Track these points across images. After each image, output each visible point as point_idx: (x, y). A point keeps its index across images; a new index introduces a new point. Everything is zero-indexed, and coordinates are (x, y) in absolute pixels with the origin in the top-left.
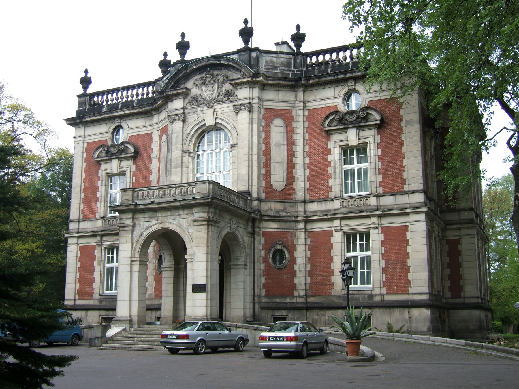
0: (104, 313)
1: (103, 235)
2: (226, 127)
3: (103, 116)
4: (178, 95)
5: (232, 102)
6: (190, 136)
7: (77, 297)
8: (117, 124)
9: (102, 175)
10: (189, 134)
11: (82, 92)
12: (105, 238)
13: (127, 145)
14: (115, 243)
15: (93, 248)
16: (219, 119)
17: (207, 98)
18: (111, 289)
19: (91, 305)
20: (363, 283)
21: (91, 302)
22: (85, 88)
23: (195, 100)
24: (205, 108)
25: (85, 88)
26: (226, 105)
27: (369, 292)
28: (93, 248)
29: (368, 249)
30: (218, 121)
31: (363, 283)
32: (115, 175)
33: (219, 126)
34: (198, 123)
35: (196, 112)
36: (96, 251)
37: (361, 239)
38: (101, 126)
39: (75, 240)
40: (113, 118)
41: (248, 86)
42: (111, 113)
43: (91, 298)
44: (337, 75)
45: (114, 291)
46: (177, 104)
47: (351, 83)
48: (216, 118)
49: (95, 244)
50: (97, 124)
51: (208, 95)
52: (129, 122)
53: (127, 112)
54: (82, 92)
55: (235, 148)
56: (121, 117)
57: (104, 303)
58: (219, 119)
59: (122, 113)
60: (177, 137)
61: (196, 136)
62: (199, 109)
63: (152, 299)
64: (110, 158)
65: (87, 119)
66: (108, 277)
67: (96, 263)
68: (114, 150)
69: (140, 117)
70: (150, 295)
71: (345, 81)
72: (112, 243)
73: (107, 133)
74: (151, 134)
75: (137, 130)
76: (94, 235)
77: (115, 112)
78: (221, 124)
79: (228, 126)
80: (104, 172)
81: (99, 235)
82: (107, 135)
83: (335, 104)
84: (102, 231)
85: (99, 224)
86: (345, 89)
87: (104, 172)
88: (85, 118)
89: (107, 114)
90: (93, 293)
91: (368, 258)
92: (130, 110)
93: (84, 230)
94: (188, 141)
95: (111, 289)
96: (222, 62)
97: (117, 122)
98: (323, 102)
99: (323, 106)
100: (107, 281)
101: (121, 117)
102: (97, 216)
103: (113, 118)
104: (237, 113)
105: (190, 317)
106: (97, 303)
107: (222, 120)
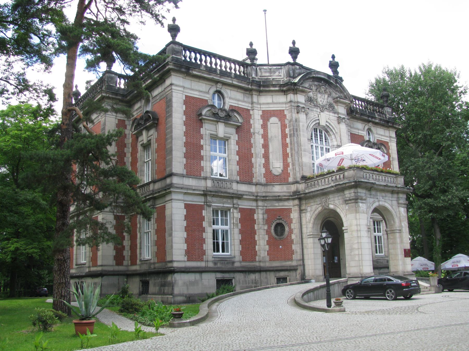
0: (219, 276)
1: (214, 196)
3: (212, 77)
4: (303, 91)
5: (335, 113)
7: (186, 259)
8: (218, 89)
9: (206, 134)
11: (170, 39)
12: (215, 199)
13: (236, 114)
14: (224, 205)
15: (201, 208)
17: (321, 103)
18: (218, 251)
19: (202, 268)
20: (380, 253)
21: (203, 264)
22: (174, 36)
23: (310, 100)
24: (319, 110)
25: (174, 36)
26: (331, 114)
27: (386, 258)
28: (201, 208)
29: (380, 232)
31: (380, 253)
32: (221, 139)
33: (326, 127)
34: (315, 121)
35: (313, 111)
36: (203, 211)
37: (377, 226)
38: (200, 84)
39: (180, 197)
40: (217, 82)
41: (344, 106)
42: (220, 77)
43: (202, 260)
44: (369, 117)
45: (221, 253)
46: (301, 98)
47: (370, 124)
49: (203, 204)
50: (198, 80)
51: (321, 101)
52: (229, 91)
53: (235, 83)
54: (170, 39)
56: (224, 84)
57: (219, 265)
59: (231, 82)
60: (303, 126)
62: (315, 109)
63: (265, 262)
64: (218, 120)
65: (195, 73)
66: (214, 239)
67: (205, 224)
68: (222, 114)
69: (239, 90)
70: (263, 258)
71: (369, 122)
72: (222, 205)
73: (208, 93)
74: (248, 110)
75: (237, 102)
76: (205, 194)
77: (224, 78)
78: (328, 126)
79: (333, 130)
80: (208, 132)
81: (210, 195)
82: (208, 96)
83: (363, 135)
84: (216, 192)
85: (209, 183)
86: (367, 127)
87: (208, 132)
88: (192, 70)
89: (203, 73)
90: (205, 254)
91: (381, 237)
92: (238, 82)
93: (196, 188)
95: (218, 251)
96: (331, 81)
97: (219, 86)
98: (357, 131)
99: (357, 134)
100: (214, 243)
101: (224, 84)
102: (202, 175)
103: (217, 82)
104: (339, 123)
105: (349, 274)
106: (211, 265)
107: (330, 124)
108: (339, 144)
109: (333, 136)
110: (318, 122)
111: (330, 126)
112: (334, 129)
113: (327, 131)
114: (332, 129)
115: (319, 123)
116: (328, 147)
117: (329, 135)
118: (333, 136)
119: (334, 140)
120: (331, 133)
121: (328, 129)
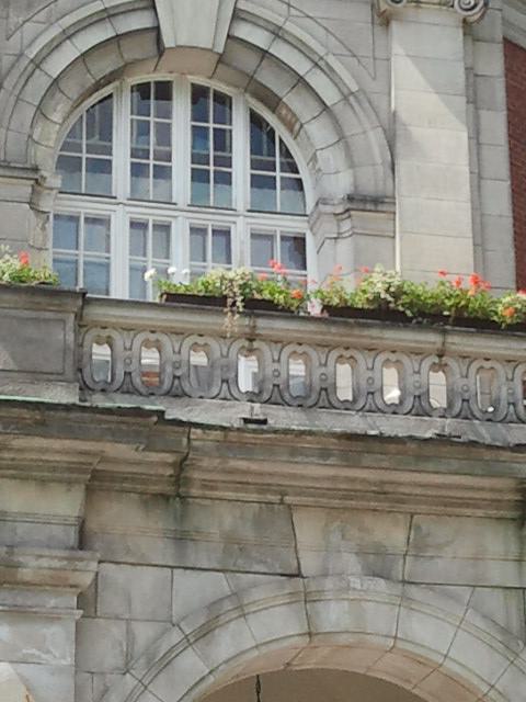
2: (300, 82)
6: (40, 83)
10: (38, 63)
16: (254, 20)
30: (244, 31)
48: (237, 15)
55: (374, 220)
58: (254, 20)
61: (72, 89)
78: (264, 54)
79: (318, 81)
94: (31, 112)
107: (277, 33)
108: (371, 183)
109: (318, 131)
110: (140, 21)
111: (281, 51)
112: (329, 72)
113: (273, 103)
114: (301, 66)
115: (157, 29)
116: (295, 226)
117: (290, 127)
118: (318, 131)
119: (332, 159)
120: (295, 102)
121: (267, 78)
